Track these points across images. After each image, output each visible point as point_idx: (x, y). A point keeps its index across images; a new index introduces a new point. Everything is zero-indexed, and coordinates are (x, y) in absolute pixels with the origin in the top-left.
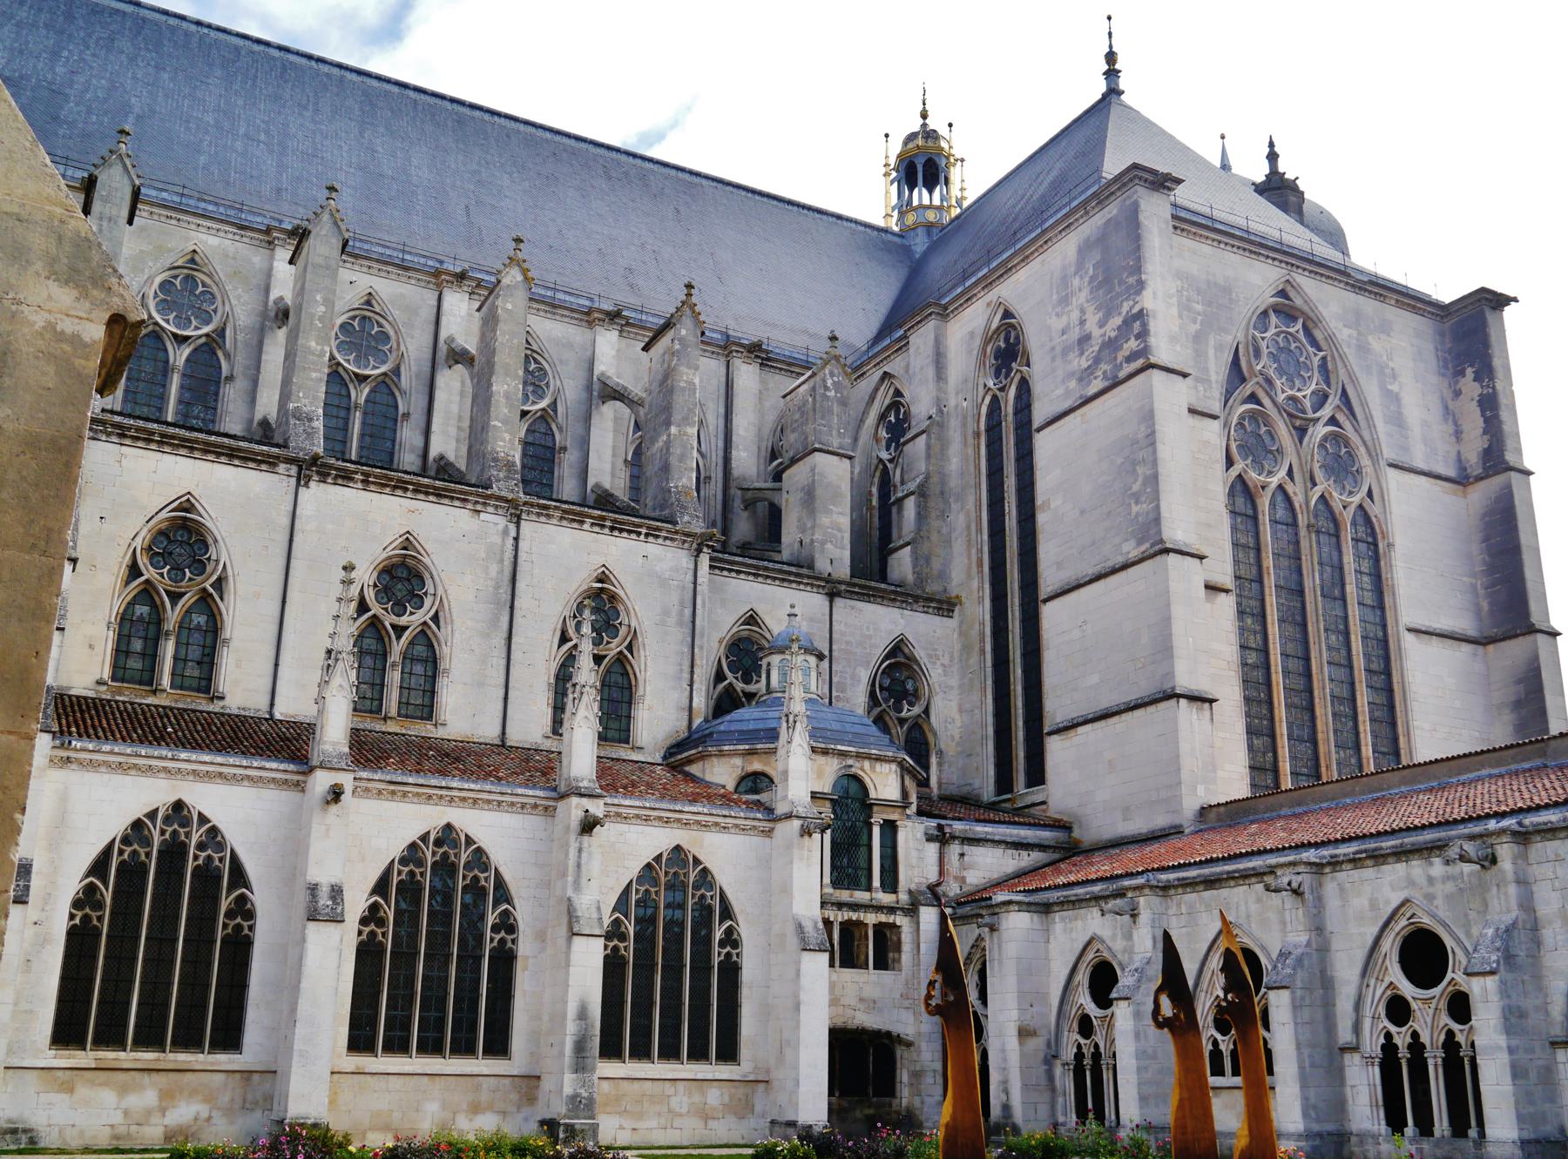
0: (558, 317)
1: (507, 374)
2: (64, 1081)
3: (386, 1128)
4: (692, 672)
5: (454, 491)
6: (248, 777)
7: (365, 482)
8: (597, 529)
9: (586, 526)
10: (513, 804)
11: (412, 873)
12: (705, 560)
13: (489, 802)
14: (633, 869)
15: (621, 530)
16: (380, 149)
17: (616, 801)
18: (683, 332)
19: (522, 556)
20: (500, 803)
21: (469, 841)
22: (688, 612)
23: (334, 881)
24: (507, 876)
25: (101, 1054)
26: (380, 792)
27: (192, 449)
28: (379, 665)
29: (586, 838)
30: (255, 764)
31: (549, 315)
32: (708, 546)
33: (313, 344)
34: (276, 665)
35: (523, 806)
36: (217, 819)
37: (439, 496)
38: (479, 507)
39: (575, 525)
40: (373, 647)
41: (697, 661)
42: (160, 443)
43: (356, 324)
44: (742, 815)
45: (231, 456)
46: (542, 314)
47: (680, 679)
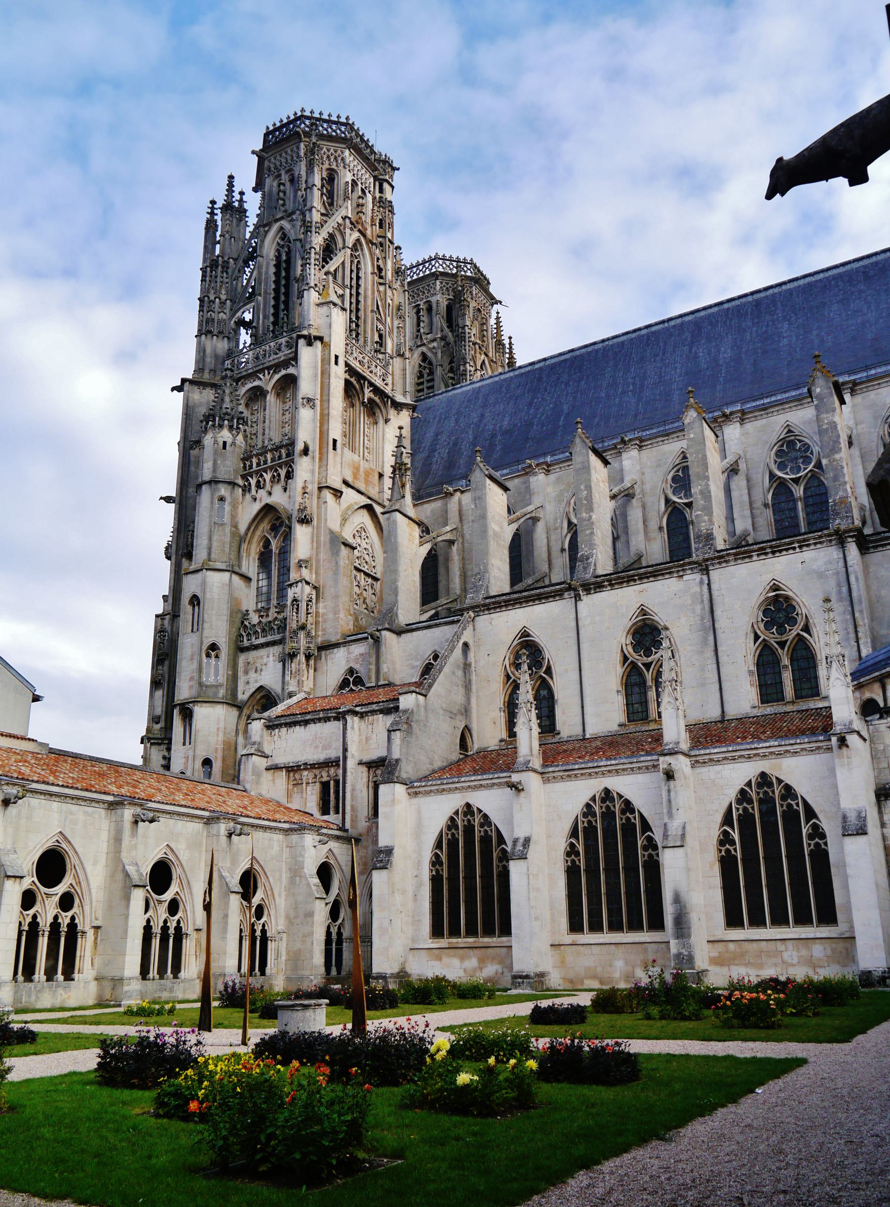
0: (806, 405)
1: (699, 479)
2: (436, 954)
3: (594, 977)
4: (856, 632)
5: (662, 570)
6: (494, 784)
7: (611, 585)
8: (763, 557)
9: (755, 558)
10: (639, 768)
11: (589, 822)
12: (852, 549)
13: (623, 770)
14: (731, 795)
15: (780, 551)
16: (701, 354)
17: (708, 751)
18: (818, 390)
19: (715, 593)
20: (632, 769)
21: (620, 796)
22: (845, 589)
23: (527, 835)
24: (645, 815)
25: (451, 940)
26: (562, 778)
27: (521, 603)
28: (643, 691)
29: (672, 783)
30: (496, 776)
31: (799, 407)
32: (850, 536)
33: (584, 515)
34: (583, 707)
35: (647, 768)
36: (486, 810)
37: (655, 576)
38: (681, 574)
39: (747, 560)
40: (638, 681)
41: (860, 622)
42: (506, 606)
43: (680, 474)
44: (806, 740)
45: (540, 599)
46: (794, 409)
47: (848, 639)
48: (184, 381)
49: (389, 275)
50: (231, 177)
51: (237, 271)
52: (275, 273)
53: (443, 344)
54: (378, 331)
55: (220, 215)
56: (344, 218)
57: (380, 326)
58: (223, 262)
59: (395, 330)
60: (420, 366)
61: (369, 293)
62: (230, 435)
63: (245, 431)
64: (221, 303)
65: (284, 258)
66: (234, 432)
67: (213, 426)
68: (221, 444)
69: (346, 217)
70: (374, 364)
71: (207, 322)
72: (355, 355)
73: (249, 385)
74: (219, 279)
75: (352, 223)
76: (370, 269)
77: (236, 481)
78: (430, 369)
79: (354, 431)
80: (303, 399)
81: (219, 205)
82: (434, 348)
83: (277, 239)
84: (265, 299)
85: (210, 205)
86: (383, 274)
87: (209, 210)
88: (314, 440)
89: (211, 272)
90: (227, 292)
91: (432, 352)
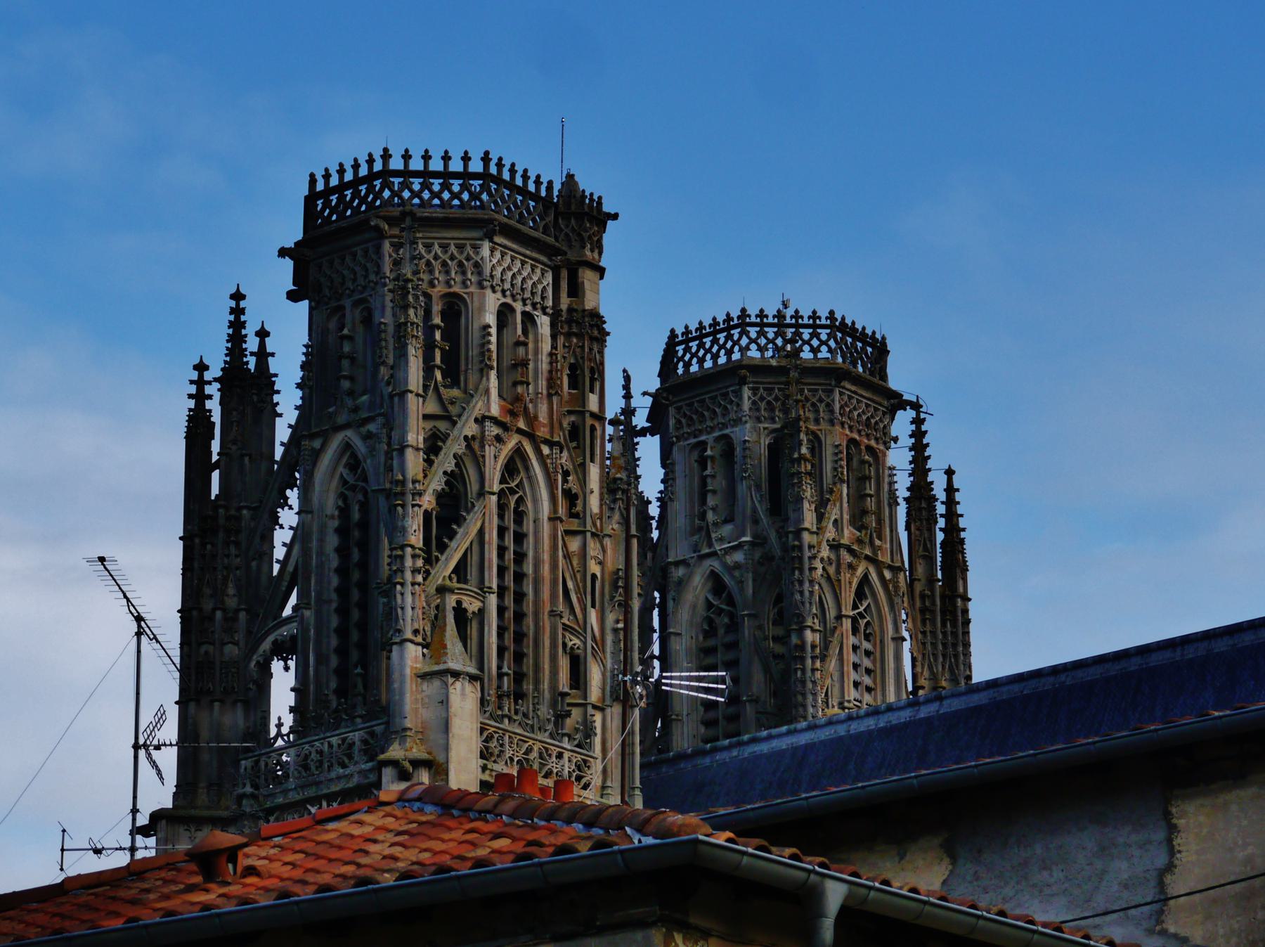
49: (594, 503)
50: (238, 296)
52: (337, 550)
53: (757, 555)
55: (217, 396)
56: (480, 421)
58: (228, 518)
59: (609, 639)
60: (709, 605)
61: (546, 570)
64: (225, 619)
65: (356, 516)
69: (484, 418)
78: (732, 616)
81: (214, 372)
82: (737, 566)
83: (341, 469)
84: (318, 614)
86: (579, 508)
89: (203, 545)
91: (733, 577)
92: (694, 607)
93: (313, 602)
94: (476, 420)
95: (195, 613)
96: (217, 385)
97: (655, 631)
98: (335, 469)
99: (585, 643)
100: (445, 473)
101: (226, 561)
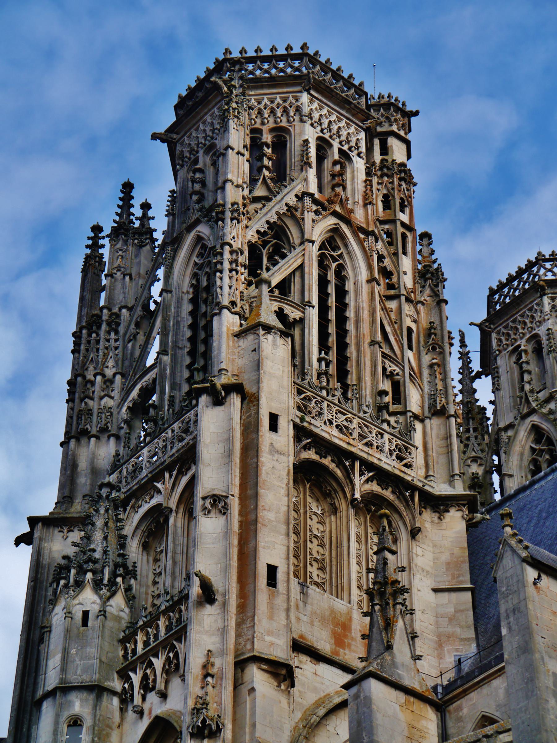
48: (33, 521)
49: (408, 281)
50: (128, 187)
51: (133, 326)
54: (389, 376)
57: (391, 367)
58: (110, 316)
59: (426, 373)
60: (533, 450)
61: (365, 314)
62: (96, 598)
63: (128, 589)
64: (105, 382)
66: (104, 591)
67: (66, 586)
68: (79, 616)
69: (305, 194)
70: (375, 430)
71: (79, 418)
72: (326, 416)
73: (145, 508)
74: (101, 346)
75: (315, 201)
76: (364, 274)
77: (107, 684)
79: (339, 556)
80: (204, 498)
81: (107, 231)
83: (194, 258)
85: (92, 235)
87: (90, 242)
88: (225, 570)
89: (90, 335)
90: (116, 362)
91: (548, 420)
92: (522, 454)
93: (169, 350)
94: (296, 196)
95: (79, 379)
96: (107, 240)
97: (496, 492)
98: (189, 259)
99: (403, 371)
100: (268, 222)
101: (107, 343)
